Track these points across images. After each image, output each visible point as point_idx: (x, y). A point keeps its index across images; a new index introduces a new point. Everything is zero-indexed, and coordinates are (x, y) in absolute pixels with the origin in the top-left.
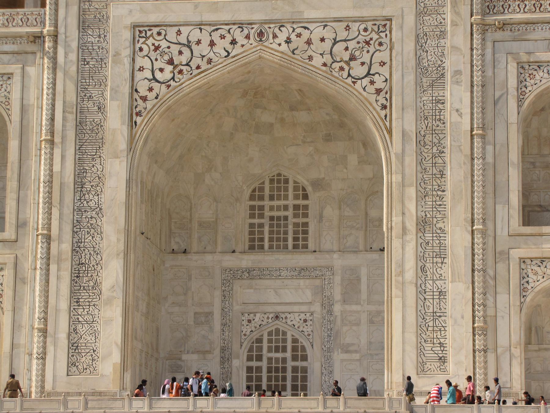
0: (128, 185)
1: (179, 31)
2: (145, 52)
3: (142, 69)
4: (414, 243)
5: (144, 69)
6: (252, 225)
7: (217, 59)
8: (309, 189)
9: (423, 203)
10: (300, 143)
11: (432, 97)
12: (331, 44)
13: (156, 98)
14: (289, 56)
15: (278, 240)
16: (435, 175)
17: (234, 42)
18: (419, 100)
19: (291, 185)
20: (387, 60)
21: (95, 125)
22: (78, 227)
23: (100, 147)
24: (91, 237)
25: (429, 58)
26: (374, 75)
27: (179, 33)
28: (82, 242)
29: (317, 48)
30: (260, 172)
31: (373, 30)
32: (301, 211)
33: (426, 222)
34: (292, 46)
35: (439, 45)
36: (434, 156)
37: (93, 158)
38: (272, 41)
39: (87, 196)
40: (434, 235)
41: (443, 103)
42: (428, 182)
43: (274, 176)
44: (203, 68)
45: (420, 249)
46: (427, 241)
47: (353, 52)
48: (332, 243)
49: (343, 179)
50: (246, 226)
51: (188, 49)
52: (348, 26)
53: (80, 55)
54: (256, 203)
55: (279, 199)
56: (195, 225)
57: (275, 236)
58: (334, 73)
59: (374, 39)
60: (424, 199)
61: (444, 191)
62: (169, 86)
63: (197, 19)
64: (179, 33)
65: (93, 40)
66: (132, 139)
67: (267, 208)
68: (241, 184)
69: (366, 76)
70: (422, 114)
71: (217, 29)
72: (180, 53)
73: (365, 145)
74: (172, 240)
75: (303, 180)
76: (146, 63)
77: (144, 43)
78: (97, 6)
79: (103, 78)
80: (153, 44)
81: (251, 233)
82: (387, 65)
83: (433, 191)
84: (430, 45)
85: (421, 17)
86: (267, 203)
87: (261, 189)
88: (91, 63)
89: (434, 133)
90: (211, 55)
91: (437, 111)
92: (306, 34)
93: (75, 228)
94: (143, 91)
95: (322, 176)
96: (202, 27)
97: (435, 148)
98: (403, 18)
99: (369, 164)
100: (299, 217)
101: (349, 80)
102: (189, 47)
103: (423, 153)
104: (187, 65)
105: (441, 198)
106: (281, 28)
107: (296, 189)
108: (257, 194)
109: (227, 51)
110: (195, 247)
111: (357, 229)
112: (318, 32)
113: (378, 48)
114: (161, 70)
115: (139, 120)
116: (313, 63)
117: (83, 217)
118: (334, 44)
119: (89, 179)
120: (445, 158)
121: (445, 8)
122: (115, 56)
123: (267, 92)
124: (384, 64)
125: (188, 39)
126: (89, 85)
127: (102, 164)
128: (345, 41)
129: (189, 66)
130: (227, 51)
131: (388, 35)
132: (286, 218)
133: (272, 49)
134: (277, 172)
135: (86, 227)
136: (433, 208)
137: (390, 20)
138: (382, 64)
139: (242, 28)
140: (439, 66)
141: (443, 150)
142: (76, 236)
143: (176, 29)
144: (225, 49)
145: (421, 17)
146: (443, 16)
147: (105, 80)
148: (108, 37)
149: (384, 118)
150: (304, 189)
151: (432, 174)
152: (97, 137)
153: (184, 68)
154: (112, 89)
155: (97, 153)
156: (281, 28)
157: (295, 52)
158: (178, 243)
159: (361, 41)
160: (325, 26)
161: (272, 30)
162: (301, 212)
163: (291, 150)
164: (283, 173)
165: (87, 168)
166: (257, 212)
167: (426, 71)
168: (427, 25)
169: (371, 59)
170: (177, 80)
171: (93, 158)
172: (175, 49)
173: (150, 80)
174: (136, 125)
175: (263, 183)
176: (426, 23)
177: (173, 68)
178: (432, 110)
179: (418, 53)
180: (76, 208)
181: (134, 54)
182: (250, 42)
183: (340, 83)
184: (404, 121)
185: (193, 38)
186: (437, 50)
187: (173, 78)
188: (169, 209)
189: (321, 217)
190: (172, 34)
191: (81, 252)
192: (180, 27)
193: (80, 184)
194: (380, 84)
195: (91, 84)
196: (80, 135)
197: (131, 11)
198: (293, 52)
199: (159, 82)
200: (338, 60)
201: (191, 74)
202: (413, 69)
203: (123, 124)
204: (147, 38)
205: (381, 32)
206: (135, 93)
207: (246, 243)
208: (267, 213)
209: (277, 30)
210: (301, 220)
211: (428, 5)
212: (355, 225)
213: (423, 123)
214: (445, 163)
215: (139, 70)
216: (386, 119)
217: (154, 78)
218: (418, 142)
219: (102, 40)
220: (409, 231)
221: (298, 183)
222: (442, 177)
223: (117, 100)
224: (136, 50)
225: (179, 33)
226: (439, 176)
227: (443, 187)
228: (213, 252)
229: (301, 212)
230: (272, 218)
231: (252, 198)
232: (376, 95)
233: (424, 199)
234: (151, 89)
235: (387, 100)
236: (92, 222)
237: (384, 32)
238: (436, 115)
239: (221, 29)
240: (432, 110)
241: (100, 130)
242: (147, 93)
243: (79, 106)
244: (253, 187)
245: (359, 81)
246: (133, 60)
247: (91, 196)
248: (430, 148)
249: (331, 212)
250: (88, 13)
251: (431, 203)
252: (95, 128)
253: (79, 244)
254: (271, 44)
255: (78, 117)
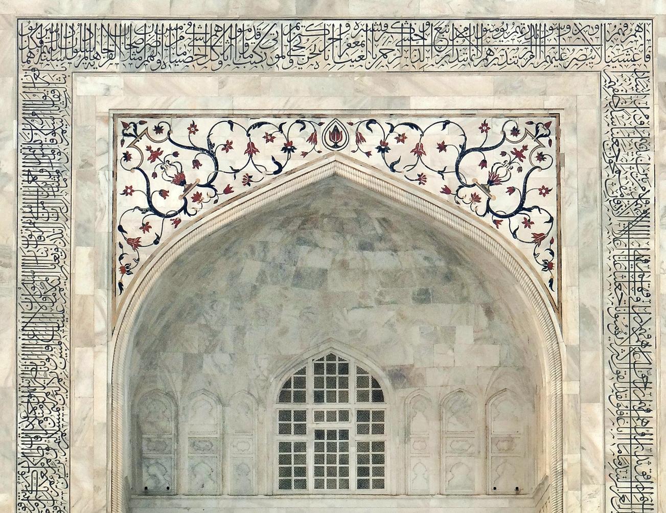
0: (110, 394)
1: (193, 125)
2: (134, 162)
3: (129, 191)
4: (600, 497)
5: (133, 191)
6: (284, 447)
7: (260, 176)
8: (385, 384)
9: (615, 431)
10: (373, 304)
11: (629, 249)
12: (457, 155)
13: (156, 242)
14: (385, 174)
15: (331, 472)
16: (634, 382)
17: (289, 148)
18: (606, 254)
19: (352, 377)
20: (552, 184)
21: (49, 288)
22: (25, 464)
23: (59, 327)
24: (48, 482)
25: (623, 182)
26: (529, 210)
27: (193, 129)
28: (32, 491)
29: (433, 161)
30: (299, 352)
31: (527, 132)
32: (371, 421)
33: (620, 463)
34: (391, 157)
35: (639, 162)
36: (632, 352)
37: (48, 346)
38: (355, 148)
39: (39, 411)
40: (634, 485)
41: (647, 261)
42: (623, 394)
43: (322, 359)
44: (237, 191)
45: (610, 508)
46: (621, 495)
47: (494, 170)
48: (427, 480)
49: (446, 368)
50: (274, 447)
51: (210, 159)
52: (485, 124)
53: (21, 164)
54: (293, 407)
55: (331, 399)
56: (185, 445)
57: (325, 465)
58: (462, 205)
59: (530, 148)
60: (616, 425)
61: (649, 411)
62: (177, 222)
63: (224, 105)
64: (193, 128)
65: (43, 138)
66: (115, 312)
67: (310, 417)
68: (266, 373)
69: (516, 212)
70: (611, 279)
71: (259, 125)
72: (196, 164)
73: (489, 312)
74: (144, 470)
75: (374, 369)
76: (138, 182)
77: (132, 145)
78: (48, 79)
79: (62, 205)
80: (149, 148)
81: (284, 460)
82: (552, 196)
83: (630, 410)
84: (624, 160)
85: (609, 112)
86: (310, 407)
87: (300, 382)
88: (39, 178)
89: (632, 311)
90: (250, 170)
91: (637, 274)
92: (413, 136)
93: (19, 467)
94: (133, 231)
95: (411, 362)
96: (233, 120)
97: (634, 338)
98: (577, 114)
99: (494, 343)
100: (368, 433)
101: (489, 218)
102: (212, 155)
103: (614, 346)
104: (208, 185)
105: (645, 422)
106: (371, 125)
107: (362, 382)
108: (292, 391)
109: (277, 163)
110: (185, 486)
111: (471, 455)
112: (435, 134)
113: (536, 163)
114: (164, 194)
115: (126, 280)
116: (427, 187)
117: (34, 447)
118: (462, 155)
119: (42, 381)
120: (652, 356)
121: (649, 99)
122: (82, 167)
123: (326, 220)
124: (548, 191)
125: (208, 140)
126: (37, 218)
127: (64, 356)
128: (481, 149)
129: (212, 187)
130: (277, 163)
131: (554, 142)
132: (344, 434)
133: (355, 161)
134: (328, 352)
135: (39, 465)
136: (631, 439)
137: (557, 116)
138: (544, 191)
139: (302, 122)
140: (640, 198)
141: (648, 340)
142: (22, 480)
143: (189, 121)
144: (273, 159)
145: (609, 113)
146: (646, 112)
147: (64, 210)
148: (68, 133)
149: (548, 285)
150: (376, 384)
151: (630, 382)
152: (54, 308)
153: (204, 191)
154: (78, 226)
155: (55, 337)
156: (370, 125)
157: (395, 167)
158: (155, 476)
159: (508, 152)
160: (447, 123)
161: (354, 127)
162: (371, 423)
163: (356, 315)
164: (338, 354)
165: (38, 362)
166: (293, 422)
167: (618, 206)
168: (618, 125)
169: (526, 182)
170: (190, 211)
171: (48, 346)
172: (187, 157)
173: (144, 211)
174: (121, 289)
175: (303, 371)
176: (616, 123)
177: (185, 191)
178: (629, 272)
179: (605, 174)
180: (20, 431)
181: (115, 165)
182: (318, 148)
183: (474, 222)
184: (583, 291)
185: (219, 140)
186: (635, 170)
187: (184, 208)
188: (138, 416)
189: (407, 432)
190: (181, 133)
191: (32, 508)
192: (195, 120)
193: (26, 389)
194: (540, 226)
195: (40, 215)
196: (24, 305)
197: (108, 89)
198: (392, 167)
199: (160, 215)
200: (470, 182)
201: (216, 201)
202: (596, 201)
203: (99, 286)
204: (137, 137)
205: (542, 136)
206: (119, 233)
207: (275, 478)
208: (311, 425)
209: (363, 129)
210: (371, 438)
211: (620, 92)
212: (466, 447)
213: (614, 295)
214: (650, 364)
215: (125, 193)
216: (551, 286)
217: (152, 208)
218: (606, 327)
219: (58, 138)
220: (592, 477)
221: (366, 373)
222: (645, 387)
223: (88, 245)
224: (119, 158)
225: (193, 128)
226: (642, 385)
227: (648, 403)
228: (217, 495)
229: (371, 423)
230: (319, 434)
231: (284, 397)
232: (534, 245)
233: (616, 424)
234: (146, 227)
235: (552, 253)
236: (48, 457)
237: (546, 136)
238: (635, 282)
239: (266, 123)
240: (629, 272)
241: (58, 296)
242: (139, 234)
243: (20, 254)
244: (284, 380)
245: (506, 220)
246: (115, 174)
247: (46, 411)
248: (626, 337)
249: (423, 424)
250: (33, 90)
251: (628, 431)
252: (50, 293)
253: (28, 494)
254: (354, 152)
255: (20, 274)
